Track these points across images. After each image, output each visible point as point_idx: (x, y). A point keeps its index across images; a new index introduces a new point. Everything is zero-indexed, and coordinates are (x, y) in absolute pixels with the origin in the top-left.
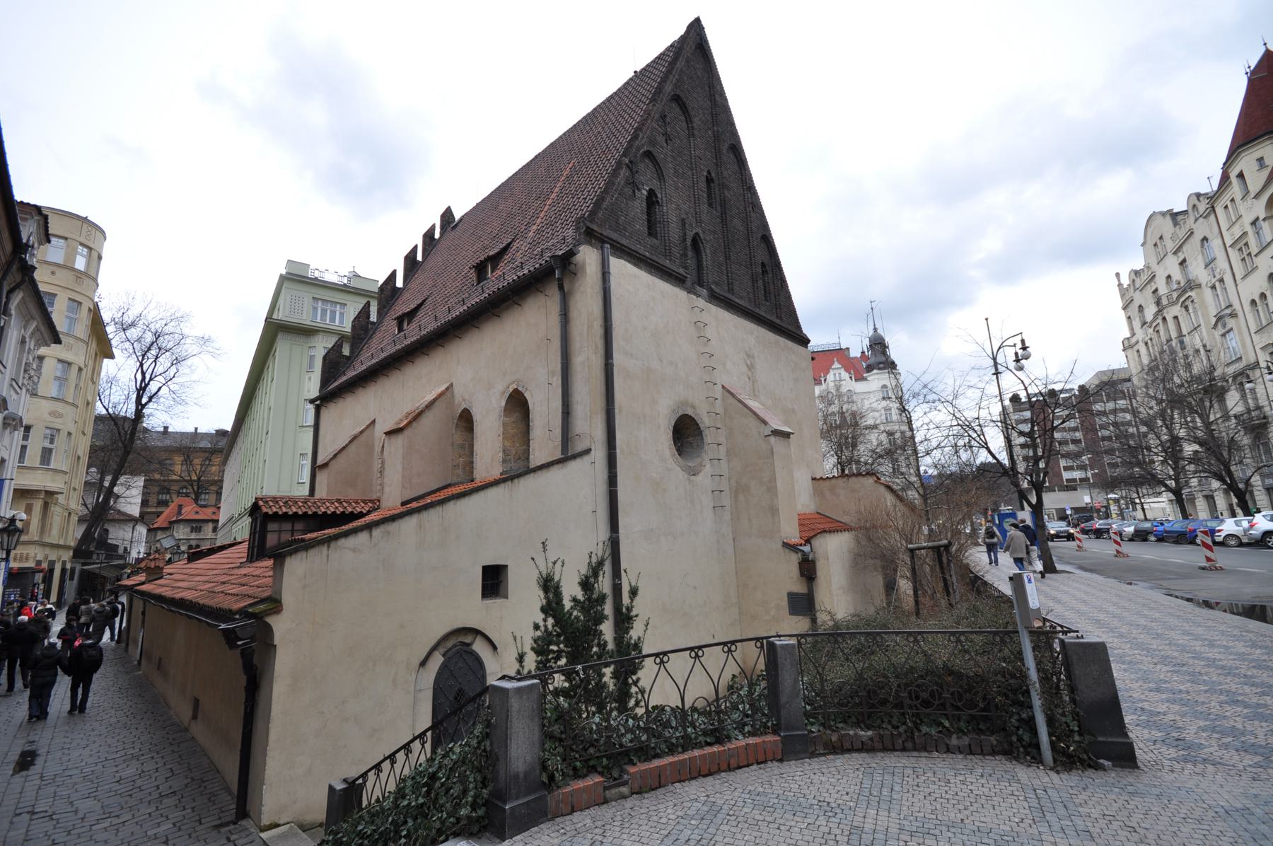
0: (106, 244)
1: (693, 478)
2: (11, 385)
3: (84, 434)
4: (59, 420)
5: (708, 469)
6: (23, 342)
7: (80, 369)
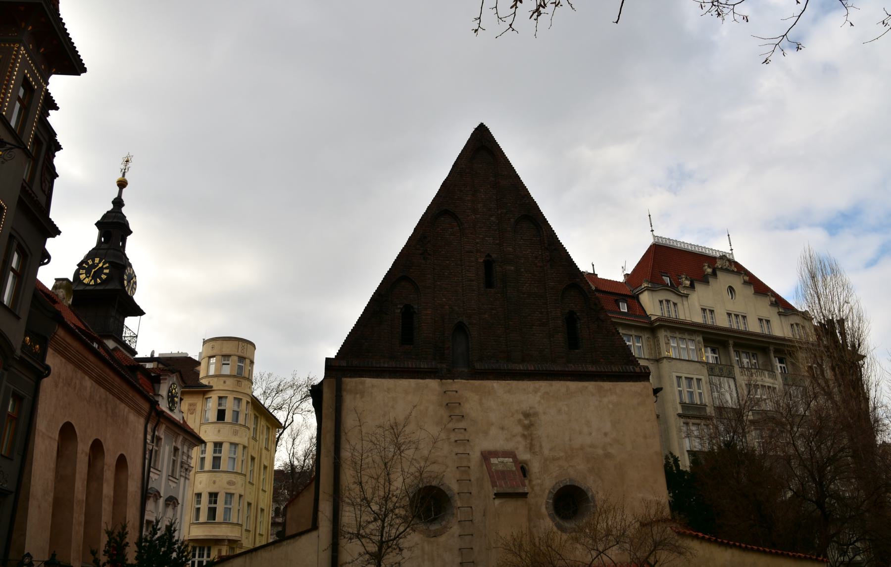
0: (256, 352)
1: (432, 539)
2: (169, 479)
3: (264, 491)
4: (233, 487)
5: (455, 529)
6: (176, 449)
7: (244, 447)
